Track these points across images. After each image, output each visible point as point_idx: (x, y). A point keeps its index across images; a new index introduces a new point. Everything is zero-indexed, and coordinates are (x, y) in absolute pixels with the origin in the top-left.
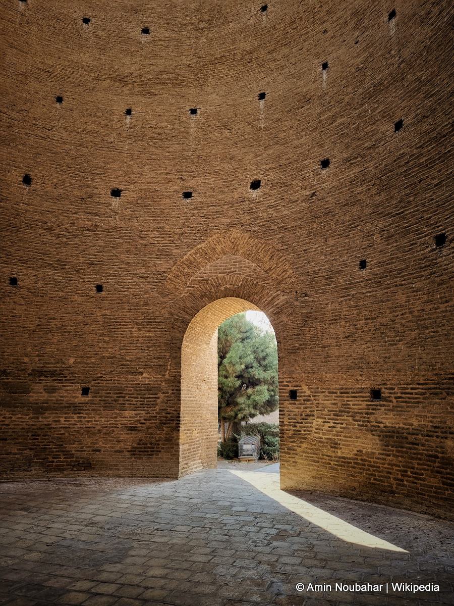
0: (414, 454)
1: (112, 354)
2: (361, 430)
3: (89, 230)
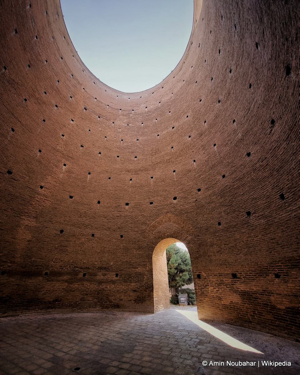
0: (257, 303)
2: (231, 292)
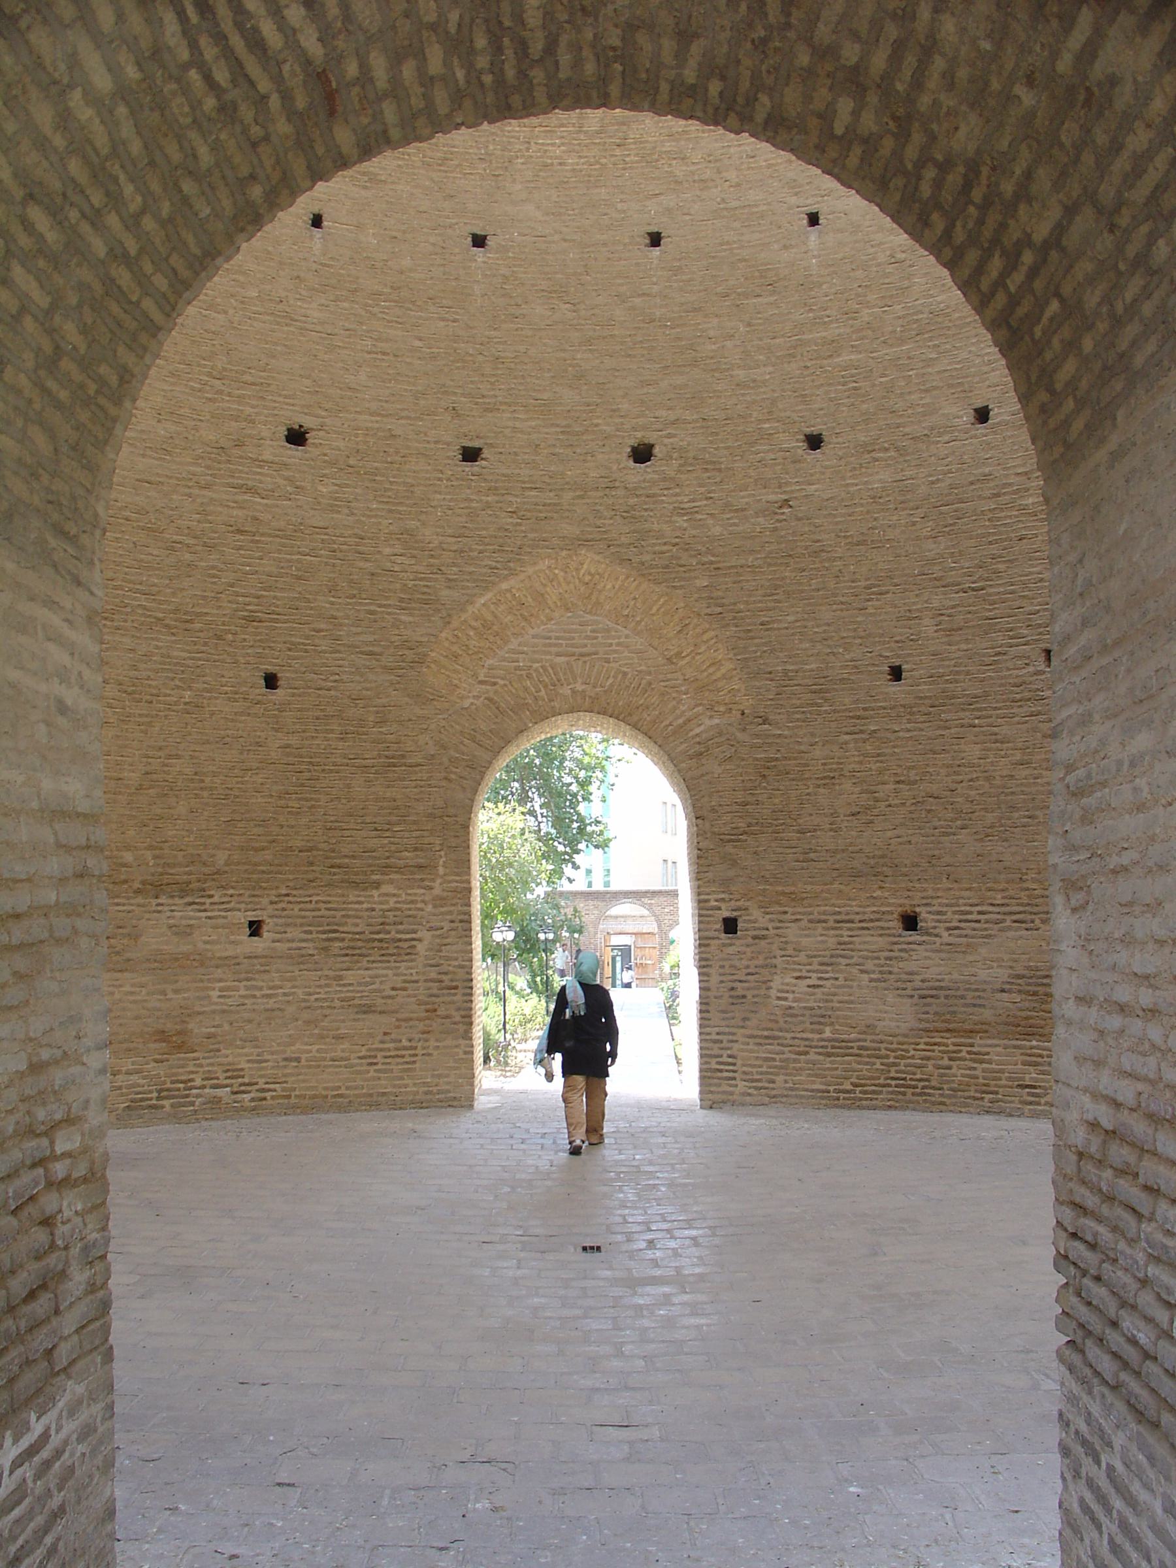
1: (308, 841)
3: (240, 532)
